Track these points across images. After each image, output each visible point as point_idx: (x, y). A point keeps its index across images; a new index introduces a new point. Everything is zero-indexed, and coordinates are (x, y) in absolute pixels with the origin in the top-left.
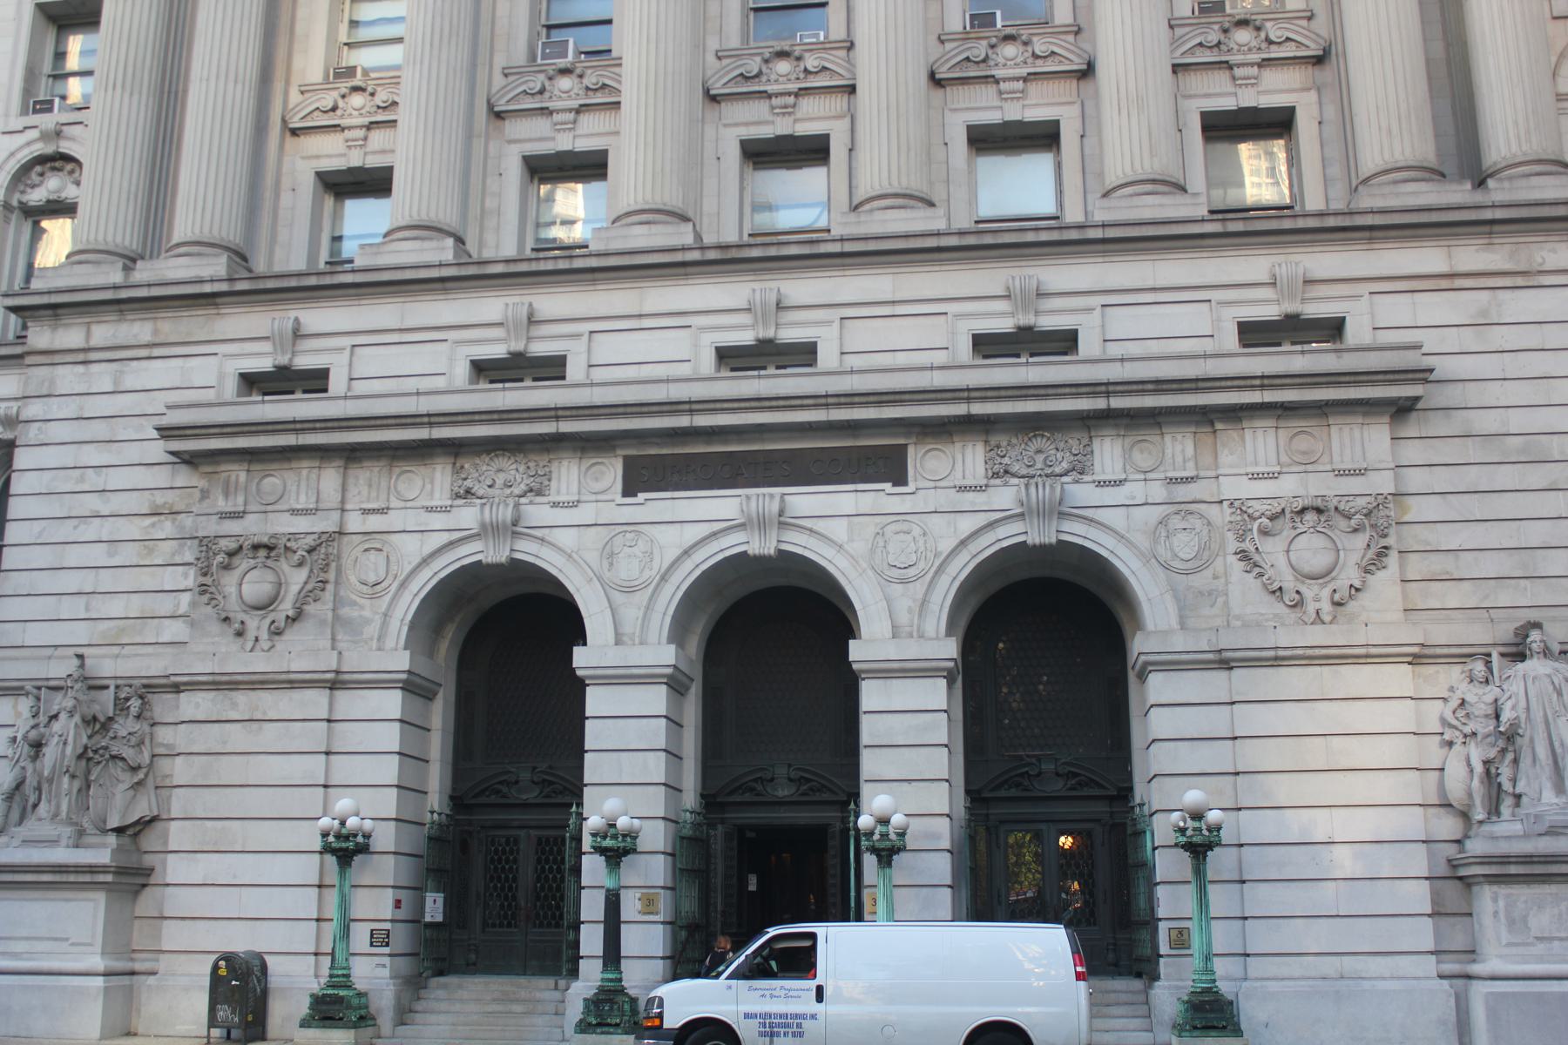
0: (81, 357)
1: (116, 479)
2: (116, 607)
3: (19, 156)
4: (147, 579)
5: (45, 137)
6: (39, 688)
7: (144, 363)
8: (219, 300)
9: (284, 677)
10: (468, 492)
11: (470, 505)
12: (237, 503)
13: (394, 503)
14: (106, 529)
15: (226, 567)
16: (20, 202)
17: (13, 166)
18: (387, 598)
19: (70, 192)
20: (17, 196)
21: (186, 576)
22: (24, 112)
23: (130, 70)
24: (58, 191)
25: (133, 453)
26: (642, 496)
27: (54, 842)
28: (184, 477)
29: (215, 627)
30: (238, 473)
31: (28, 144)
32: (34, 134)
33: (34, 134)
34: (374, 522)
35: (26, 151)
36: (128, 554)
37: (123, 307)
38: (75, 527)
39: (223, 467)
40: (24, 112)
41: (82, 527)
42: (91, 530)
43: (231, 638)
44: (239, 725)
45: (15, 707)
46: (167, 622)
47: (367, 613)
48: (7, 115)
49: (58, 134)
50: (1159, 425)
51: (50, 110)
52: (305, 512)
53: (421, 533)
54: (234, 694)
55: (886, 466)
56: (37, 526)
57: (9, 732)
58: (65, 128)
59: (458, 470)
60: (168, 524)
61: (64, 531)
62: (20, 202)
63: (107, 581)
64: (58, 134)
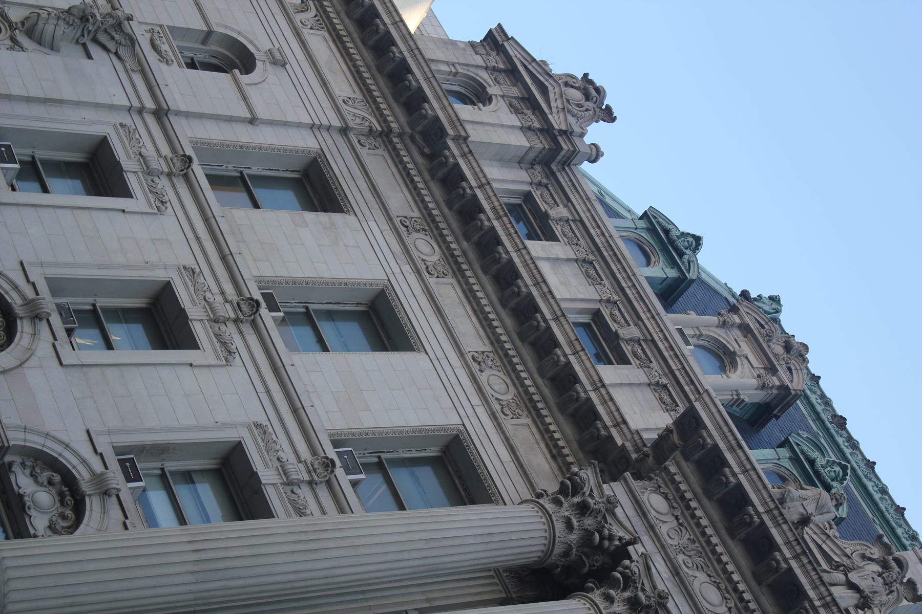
3: (67, 454)
5: (99, 480)
16: (10, 464)
17: (53, 449)
19: (39, 522)
20: (18, 459)
22: (119, 451)
23: (220, 565)
24: (37, 507)
31: (84, 462)
32: (98, 467)
33: (98, 467)
35: (75, 461)
40: (119, 451)
48: (109, 432)
49: (106, 493)
51: (129, 479)
58: (114, 499)
62: (10, 464)
64: (106, 493)
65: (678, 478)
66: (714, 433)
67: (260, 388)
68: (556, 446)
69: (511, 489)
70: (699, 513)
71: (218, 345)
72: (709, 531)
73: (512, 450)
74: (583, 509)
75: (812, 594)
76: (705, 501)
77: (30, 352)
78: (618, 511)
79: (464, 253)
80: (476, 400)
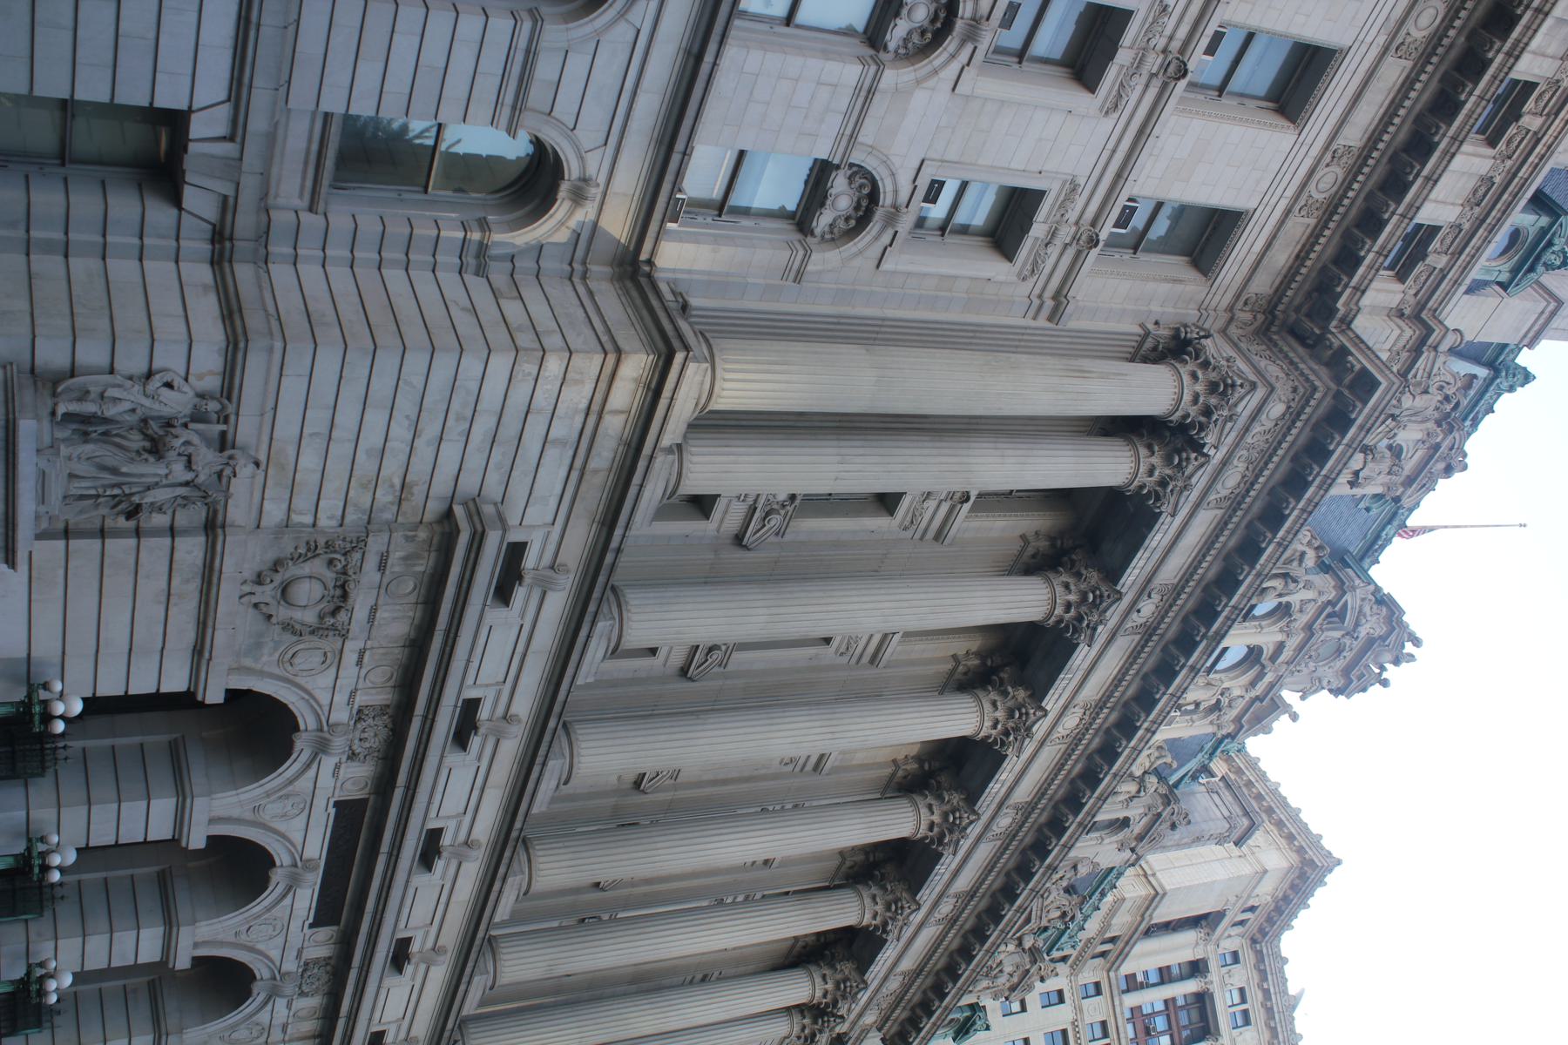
0: (595, 407)
1: (450, 452)
2: (310, 460)
4: (335, 486)
6: (226, 421)
7: (567, 461)
8: (605, 530)
9: (210, 623)
10: (359, 719)
11: (351, 718)
12: (394, 565)
13: (364, 671)
14: (399, 444)
15: (331, 562)
17: (880, 173)
18: (277, 671)
21: (331, 518)
25: (475, 461)
26: (332, 811)
27: (42, 499)
28: (434, 508)
29: (271, 556)
30: (424, 565)
31: (896, 192)
34: (350, 657)
36: (366, 465)
37: (632, 451)
38: (407, 417)
39: (433, 555)
41: (406, 423)
42: (401, 431)
43: (257, 569)
44: (164, 585)
45: (211, 373)
46: (285, 506)
47: (265, 659)
50: (324, 1018)
52: (372, 618)
53: (332, 688)
54: (198, 581)
55: (325, 913)
56: (418, 381)
57: (178, 382)
59: (383, 709)
60: (390, 498)
61: (406, 405)
63: (341, 450)
65: (1313, 403)
66: (1366, 410)
67: (1110, 146)
68: (1308, 253)
69: (1230, 276)
70: (1294, 431)
71: (1114, 93)
72: (1284, 445)
73: (1269, 245)
74: (1207, 412)
75: (1281, 533)
76: (1308, 429)
77: (936, 72)
78: (1229, 425)
79: (1451, 46)
80: (1290, 193)
